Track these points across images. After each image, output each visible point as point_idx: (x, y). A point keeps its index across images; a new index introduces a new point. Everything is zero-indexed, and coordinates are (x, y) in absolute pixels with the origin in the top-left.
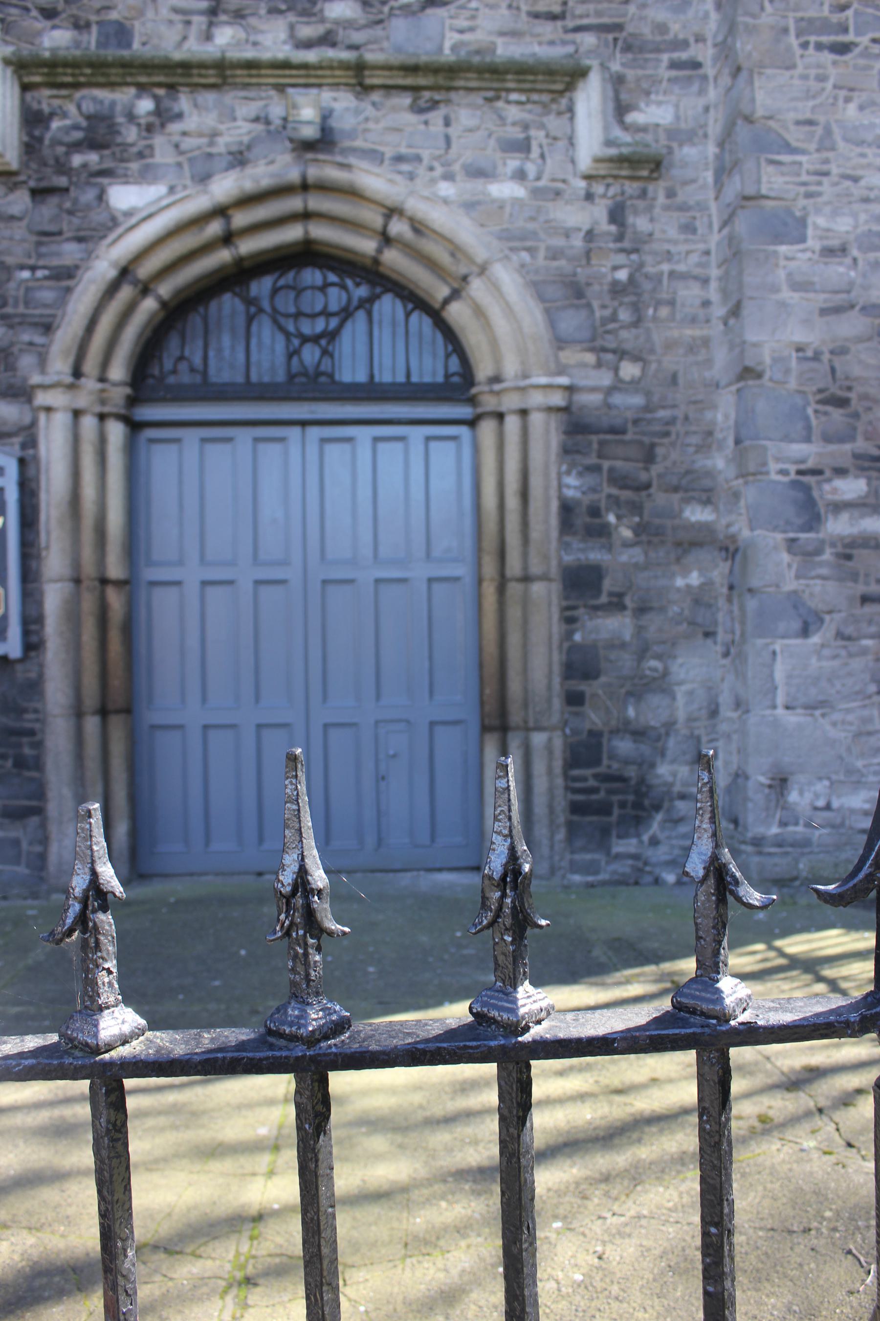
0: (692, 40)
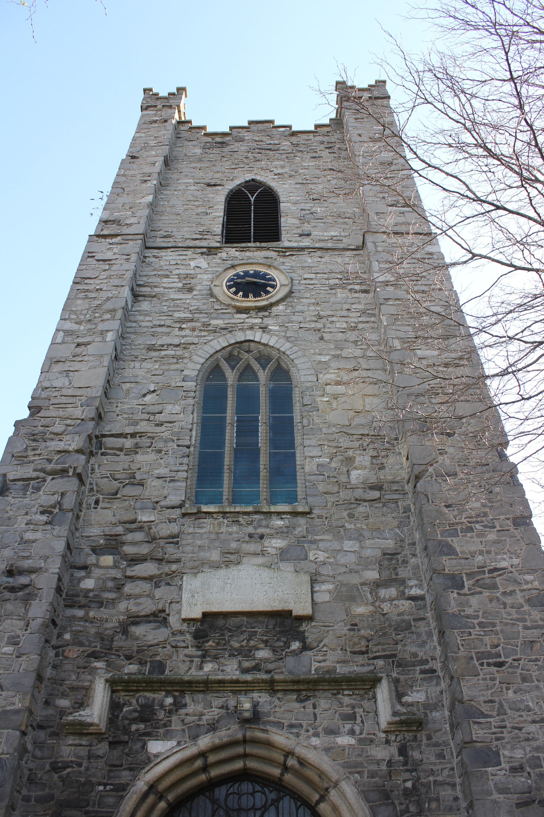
0: (430, 659)
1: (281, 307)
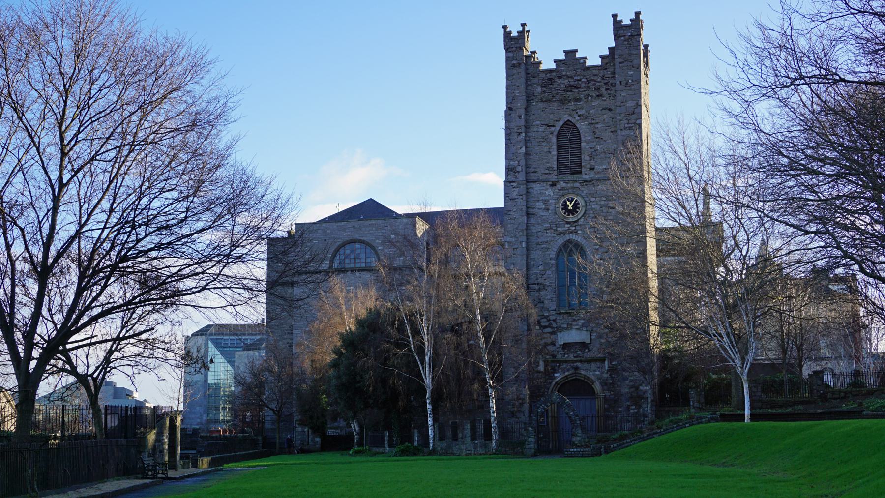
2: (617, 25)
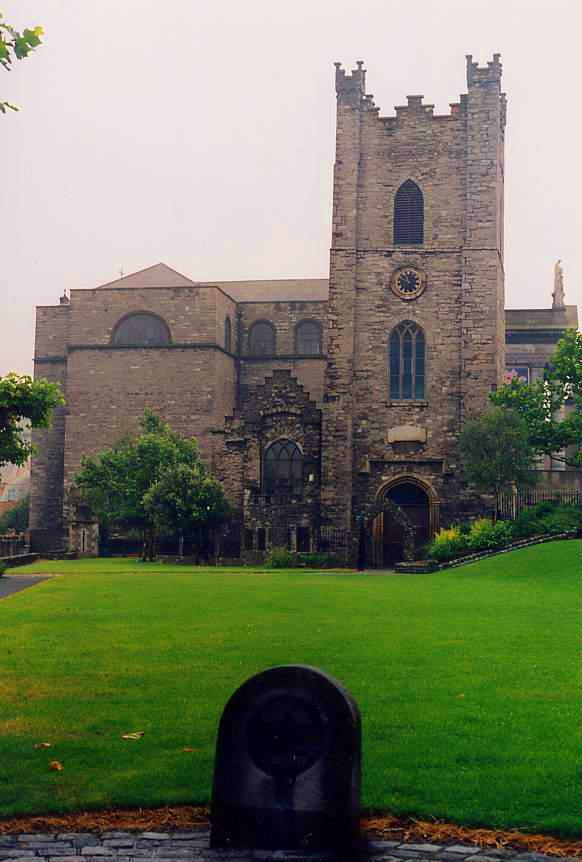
1: (421, 298)
2: (472, 67)
